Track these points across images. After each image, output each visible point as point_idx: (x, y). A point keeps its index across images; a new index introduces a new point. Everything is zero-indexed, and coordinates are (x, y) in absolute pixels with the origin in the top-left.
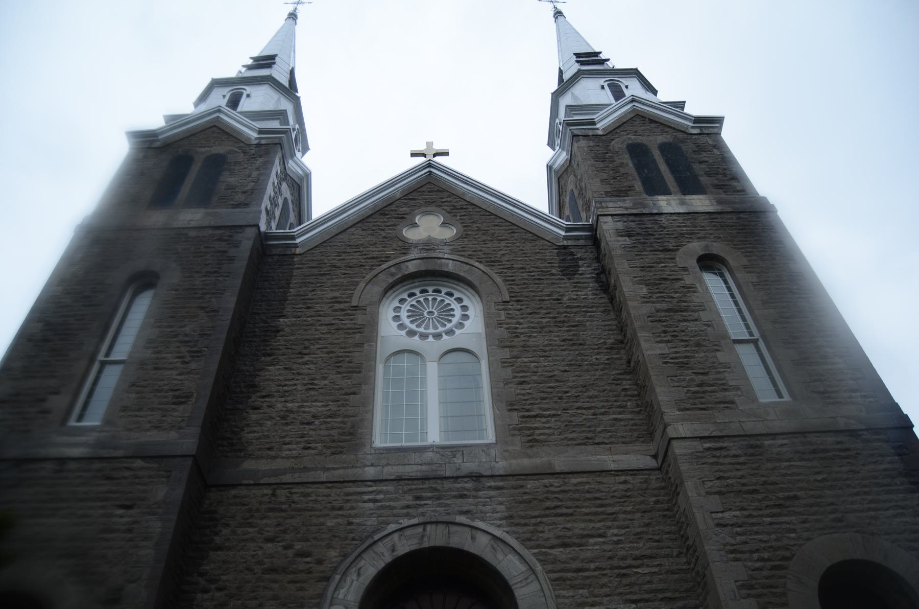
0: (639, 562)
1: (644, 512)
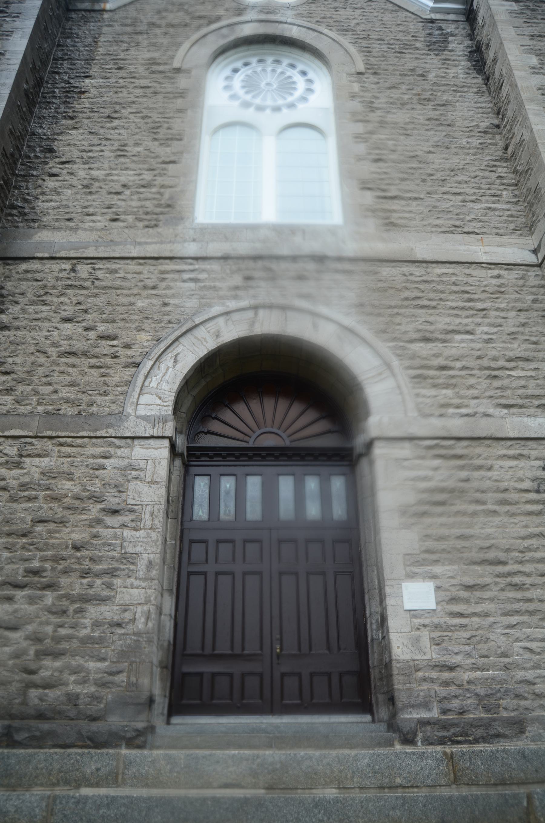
0: (512, 364)
1: (520, 310)
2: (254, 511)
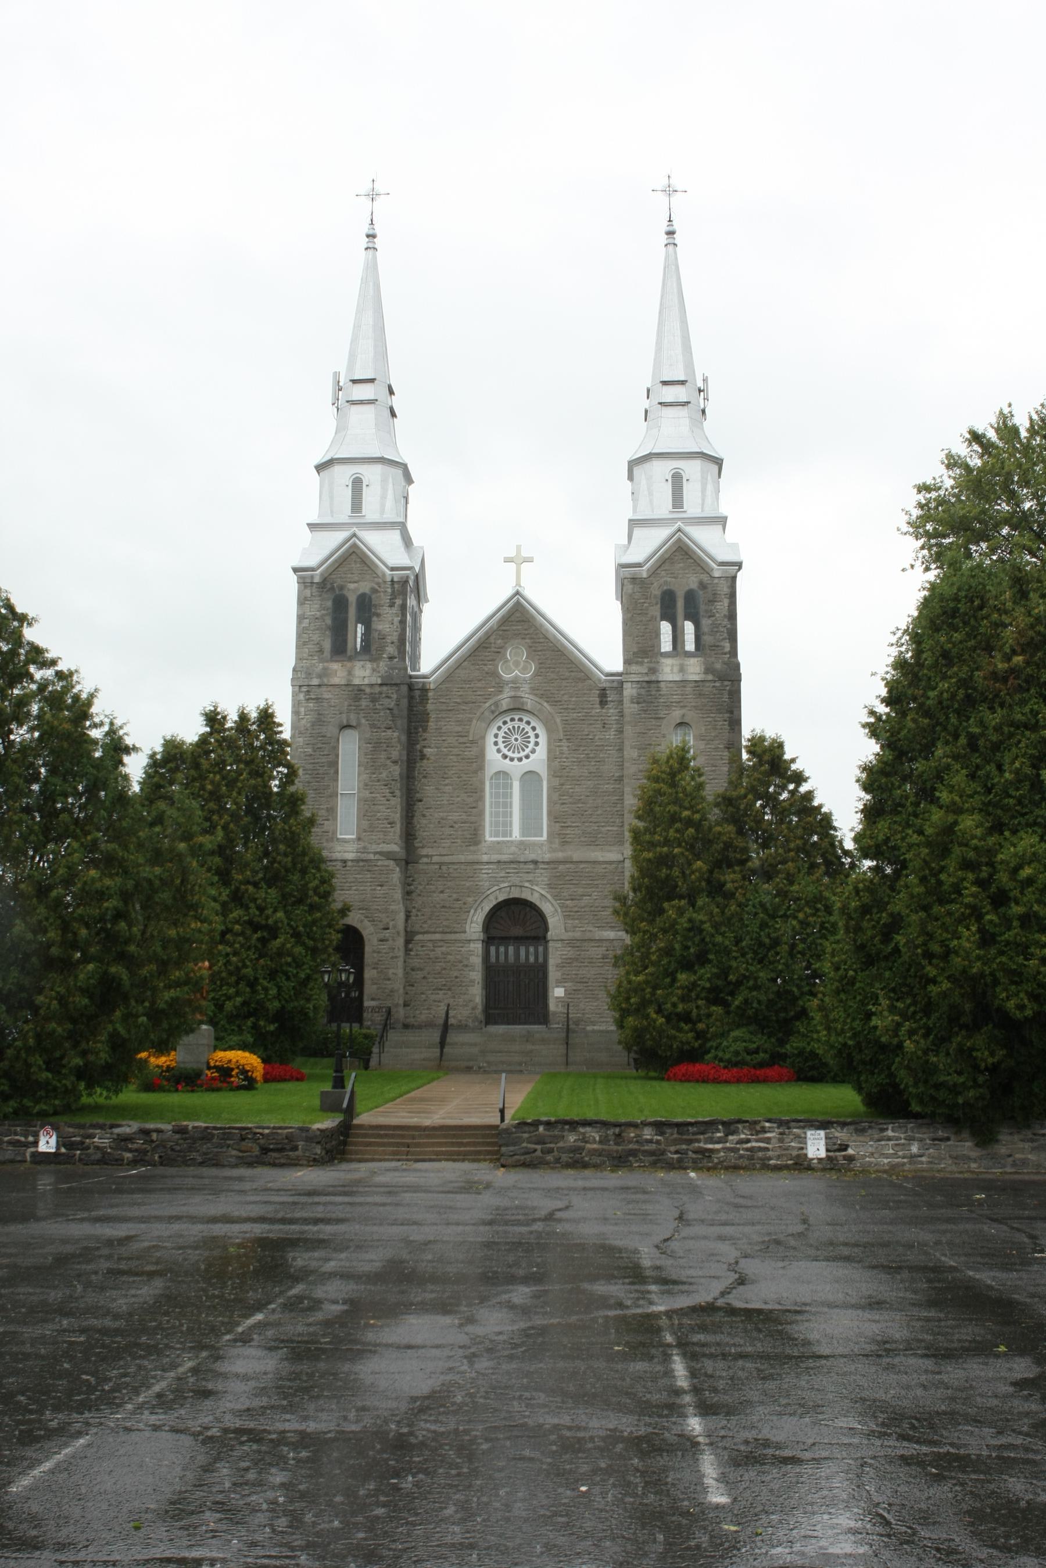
2: (511, 958)
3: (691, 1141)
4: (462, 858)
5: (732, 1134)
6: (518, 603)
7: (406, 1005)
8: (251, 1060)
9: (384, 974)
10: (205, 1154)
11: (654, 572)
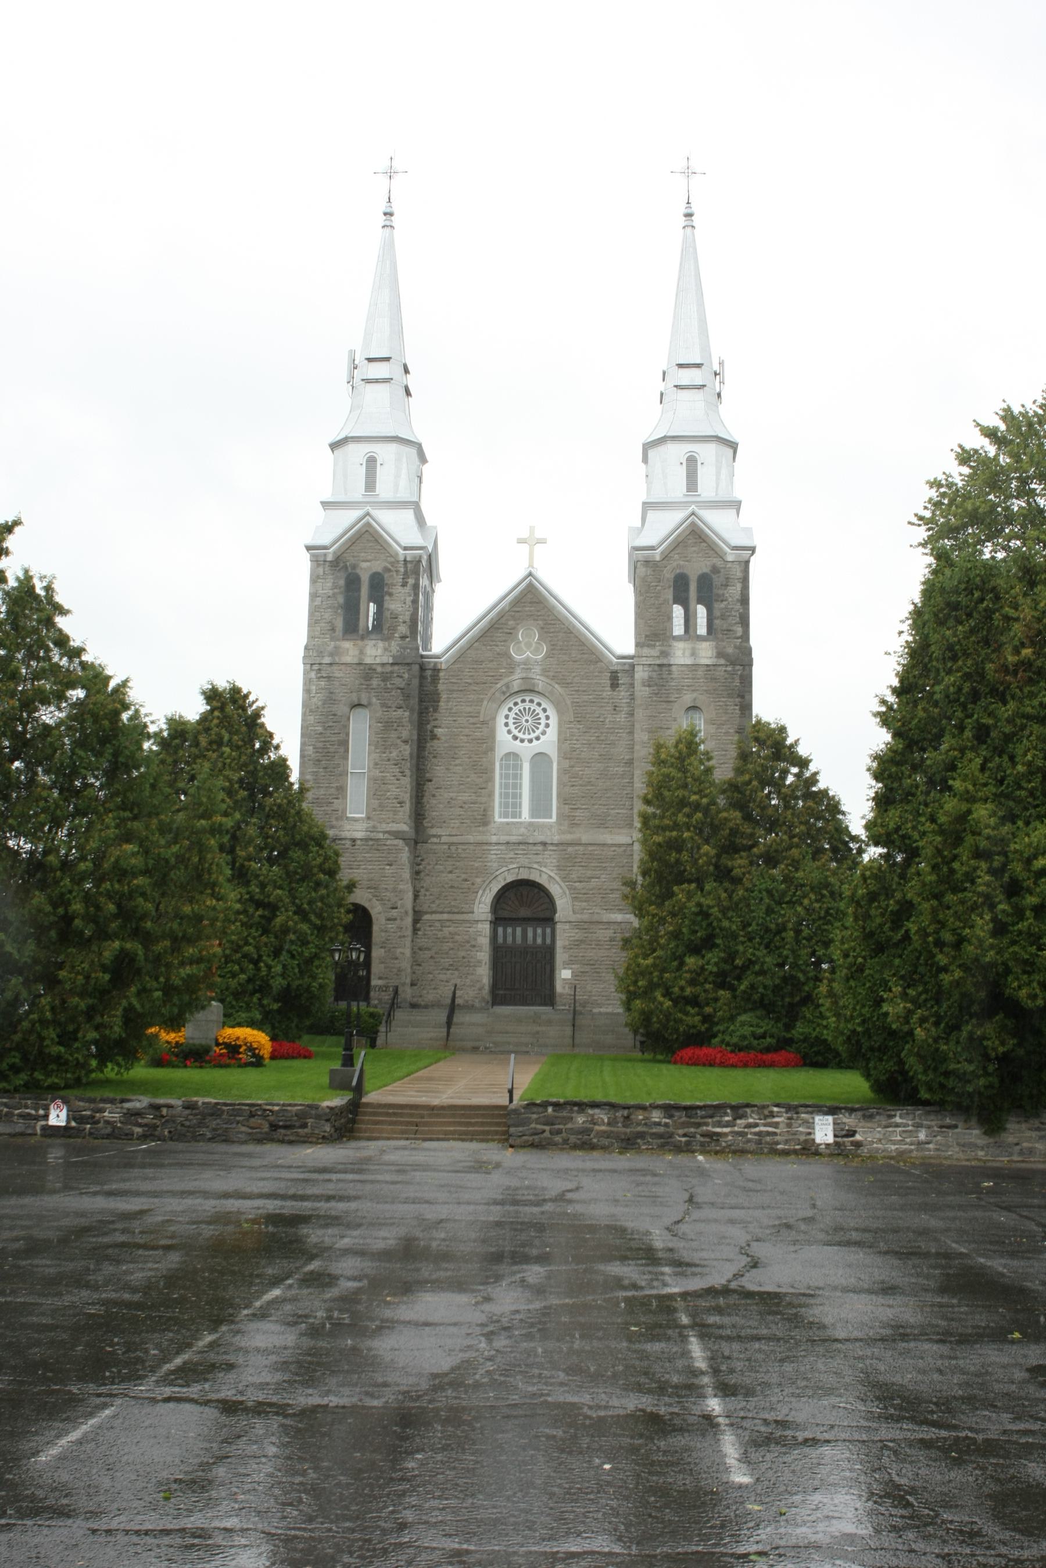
3: (699, 1125)
4: (471, 839)
5: (740, 1118)
6: (530, 586)
7: (412, 984)
8: (260, 1038)
9: (391, 955)
10: (214, 1130)
11: (666, 556)
